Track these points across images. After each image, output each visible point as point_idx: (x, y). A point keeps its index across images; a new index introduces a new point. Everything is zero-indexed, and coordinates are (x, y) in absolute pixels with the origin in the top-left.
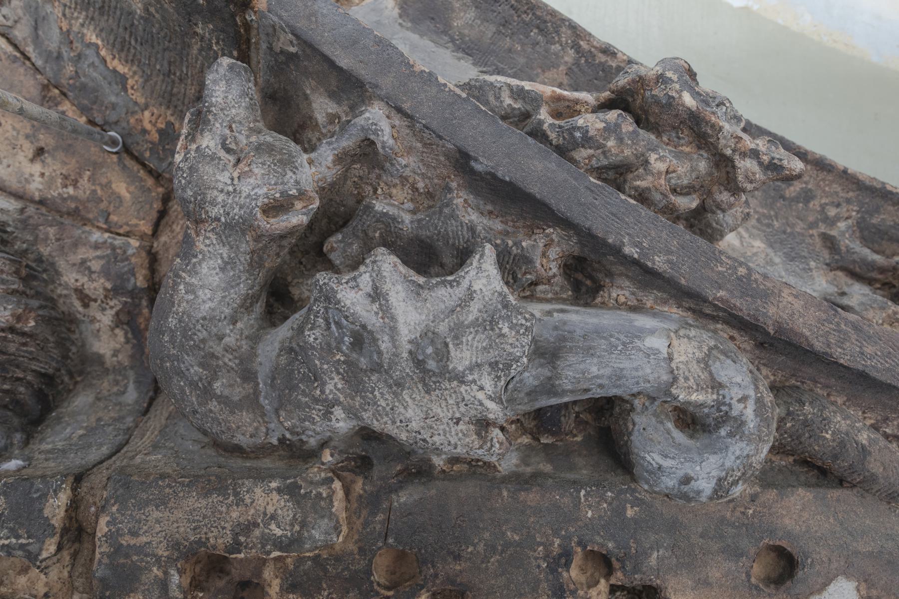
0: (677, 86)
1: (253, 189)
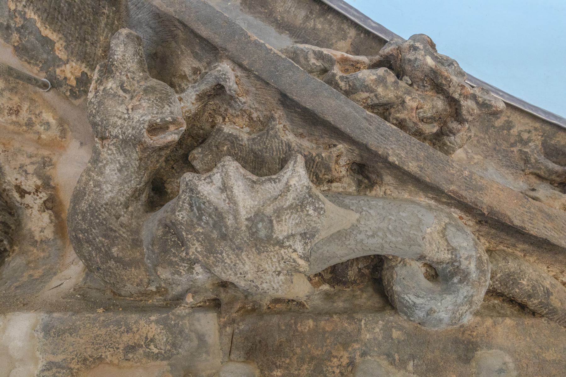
0: (423, 52)
1: (142, 116)
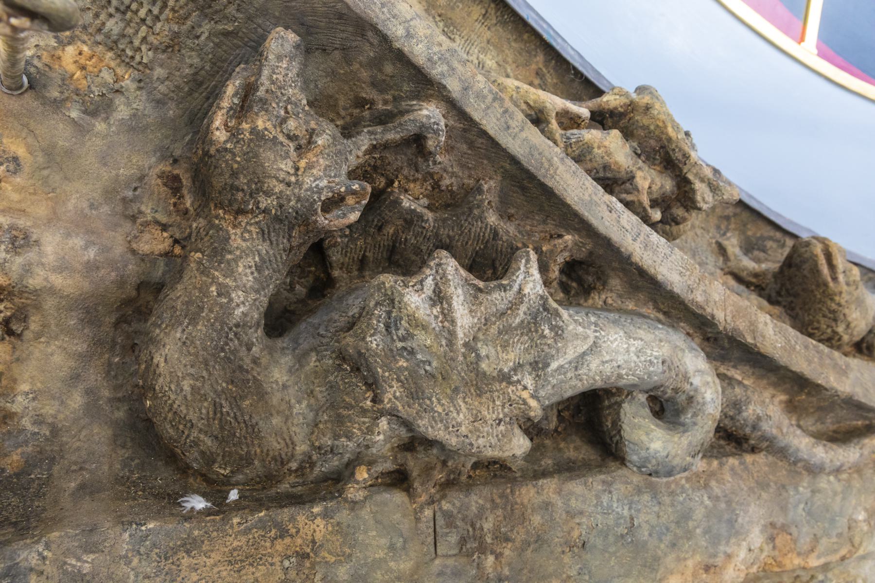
1: (315, 181)
